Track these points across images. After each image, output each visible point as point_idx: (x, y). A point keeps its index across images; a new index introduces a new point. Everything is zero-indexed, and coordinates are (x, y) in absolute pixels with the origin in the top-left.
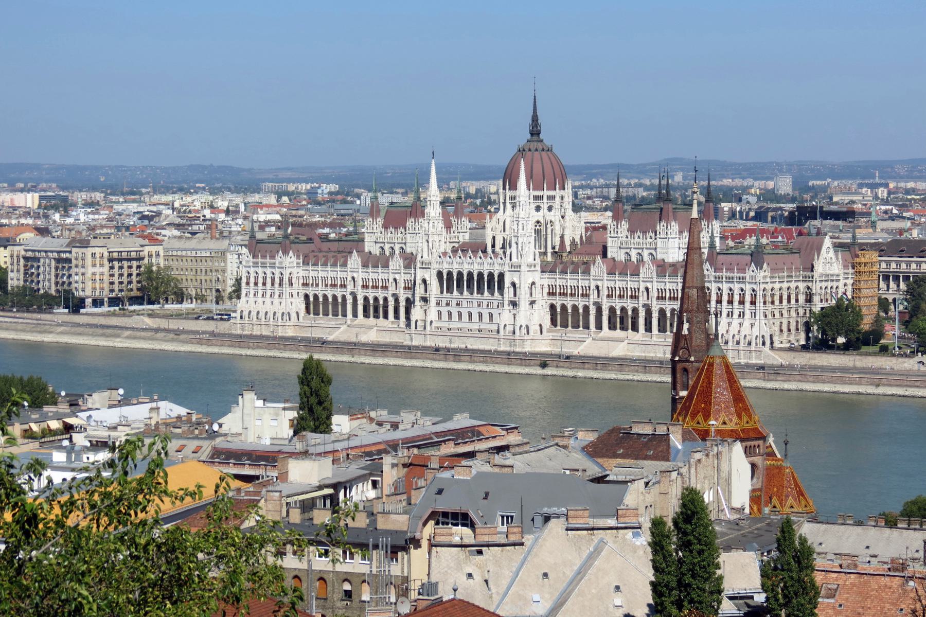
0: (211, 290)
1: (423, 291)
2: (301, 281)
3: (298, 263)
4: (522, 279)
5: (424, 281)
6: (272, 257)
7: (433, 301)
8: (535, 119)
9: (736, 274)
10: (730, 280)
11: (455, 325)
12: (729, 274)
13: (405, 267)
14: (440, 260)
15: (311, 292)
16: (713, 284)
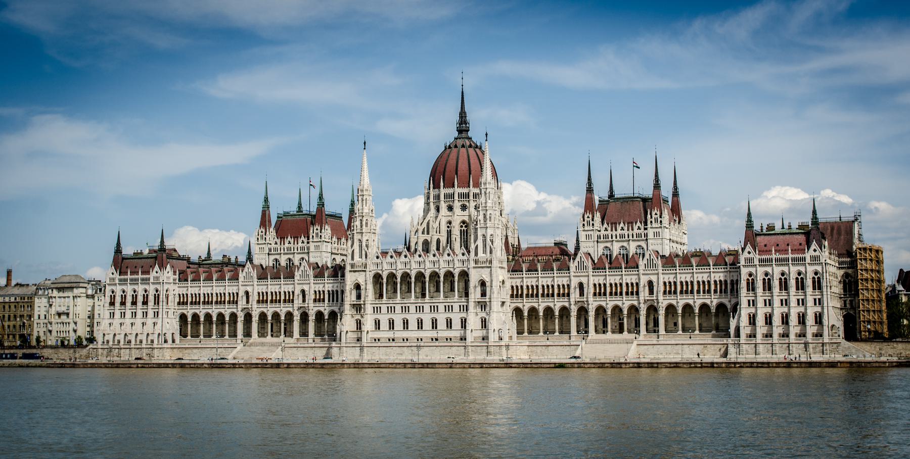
0: (14, 336)
1: (354, 297)
2: (177, 300)
3: (174, 280)
4: (494, 275)
5: (358, 287)
6: (148, 273)
7: (369, 309)
8: (463, 114)
9: (790, 256)
10: (781, 262)
11: (399, 333)
12: (779, 256)
13: (316, 277)
14: (379, 261)
15: (189, 311)
16: (759, 269)
